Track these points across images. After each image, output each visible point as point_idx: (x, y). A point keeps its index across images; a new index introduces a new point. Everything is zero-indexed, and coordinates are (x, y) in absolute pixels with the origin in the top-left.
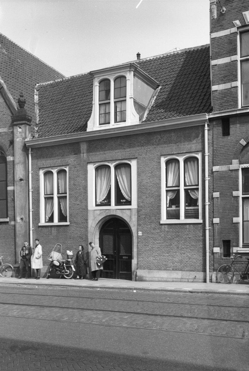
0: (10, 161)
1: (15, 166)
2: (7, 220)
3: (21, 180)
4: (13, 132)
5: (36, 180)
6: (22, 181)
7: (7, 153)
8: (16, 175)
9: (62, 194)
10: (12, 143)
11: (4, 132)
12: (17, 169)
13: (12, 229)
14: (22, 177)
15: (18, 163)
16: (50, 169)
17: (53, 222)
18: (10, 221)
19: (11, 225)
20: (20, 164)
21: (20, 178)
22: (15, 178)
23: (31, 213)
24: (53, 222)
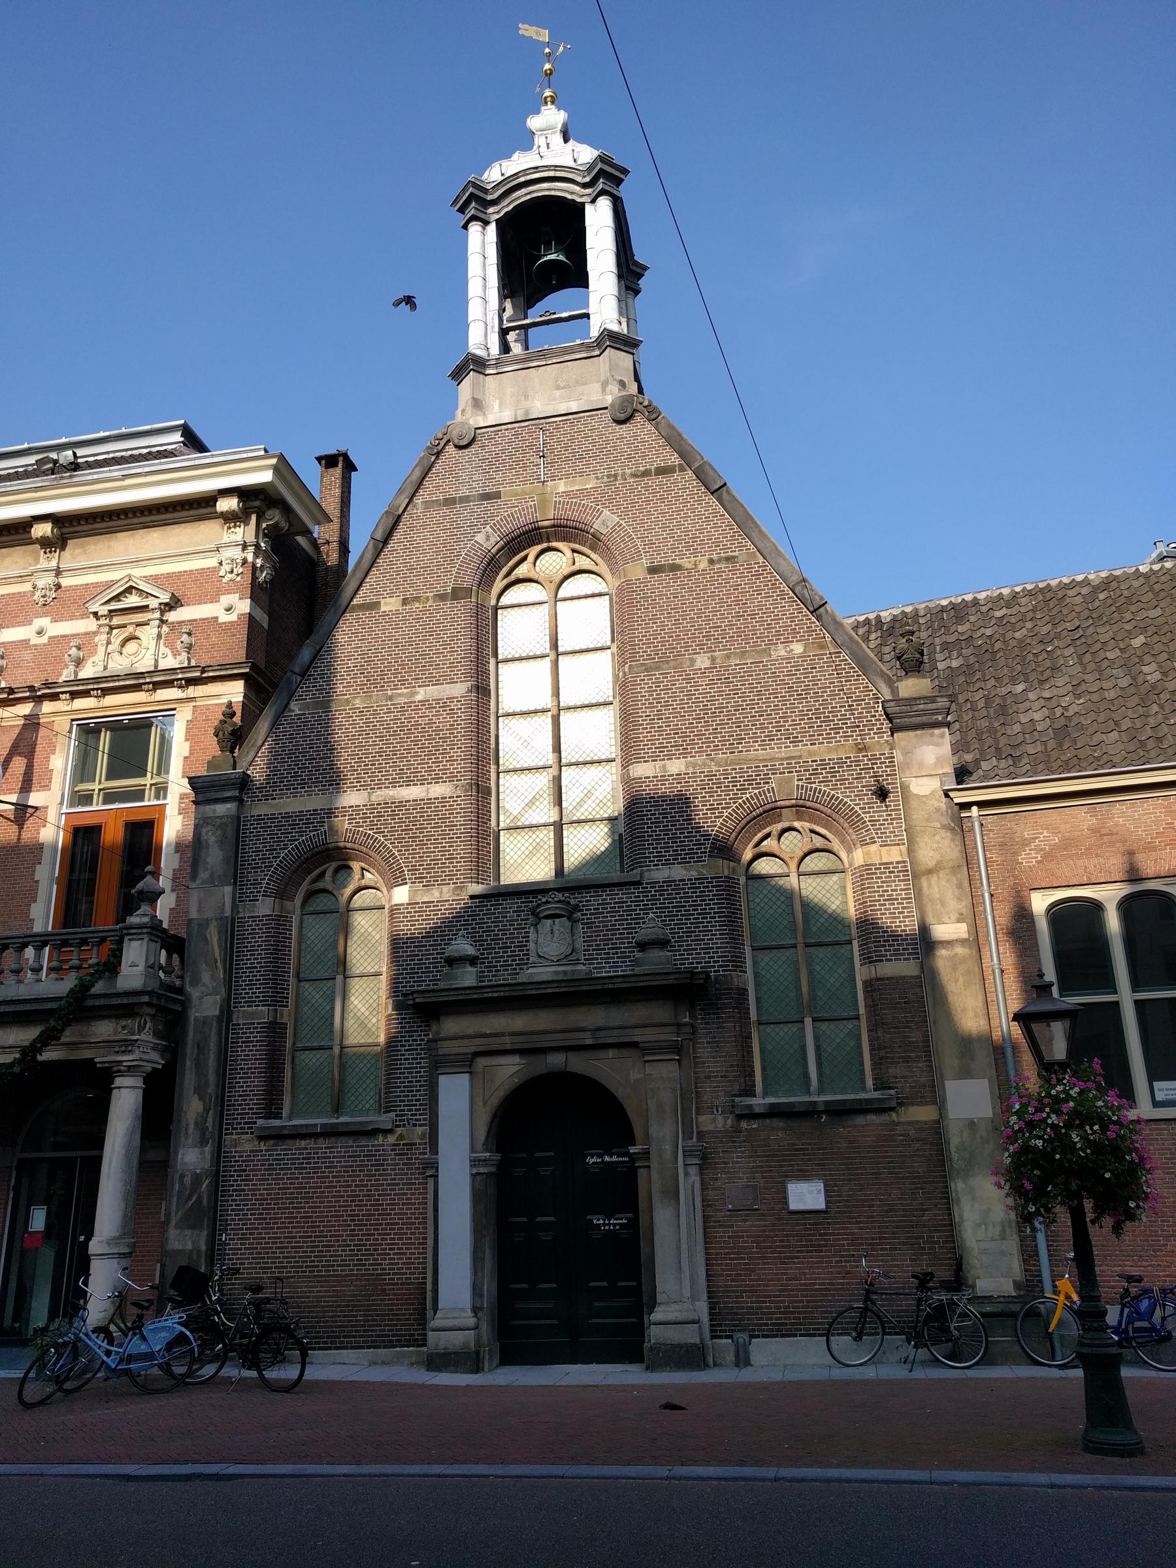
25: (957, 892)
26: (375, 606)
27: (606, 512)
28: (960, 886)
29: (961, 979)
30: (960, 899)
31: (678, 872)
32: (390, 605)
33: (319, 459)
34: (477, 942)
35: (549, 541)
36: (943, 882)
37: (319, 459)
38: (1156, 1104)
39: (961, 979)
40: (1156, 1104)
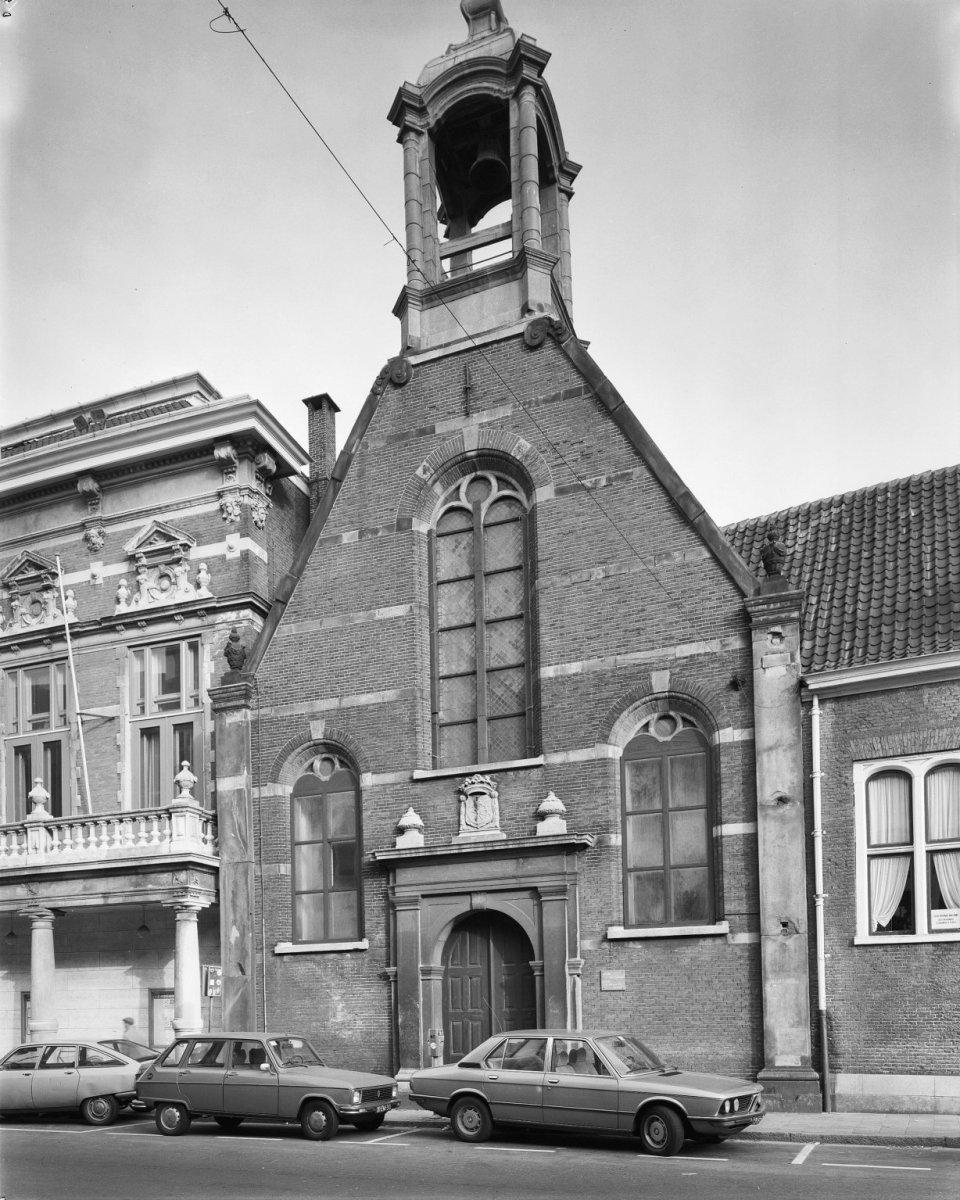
0: (731, 745)
1: (758, 758)
2: (722, 927)
3: (782, 800)
4: (748, 653)
5: (842, 795)
6: (787, 807)
7: (720, 720)
8: (762, 786)
9: (939, 841)
10: (743, 683)
11: (706, 654)
12: (766, 765)
13: (740, 958)
14: (785, 791)
15: (770, 749)
16: (898, 763)
17: (913, 932)
18: (731, 932)
19: (737, 945)
20: (780, 750)
21: (778, 795)
22: (759, 795)
23: (820, 903)
24: (913, 932)
25: (792, 765)
26: (337, 539)
27: (522, 441)
28: (794, 760)
29: (787, 835)
30: (792, 770)
31: (578, 756)
32: (349, 537)
33: (306, 402)
34: (423, 816)
35: (476, 470)
36: (781, 757)
37: (306, 402)
38: (931, 931)
39: (787, 835)
40: (931, 931)
